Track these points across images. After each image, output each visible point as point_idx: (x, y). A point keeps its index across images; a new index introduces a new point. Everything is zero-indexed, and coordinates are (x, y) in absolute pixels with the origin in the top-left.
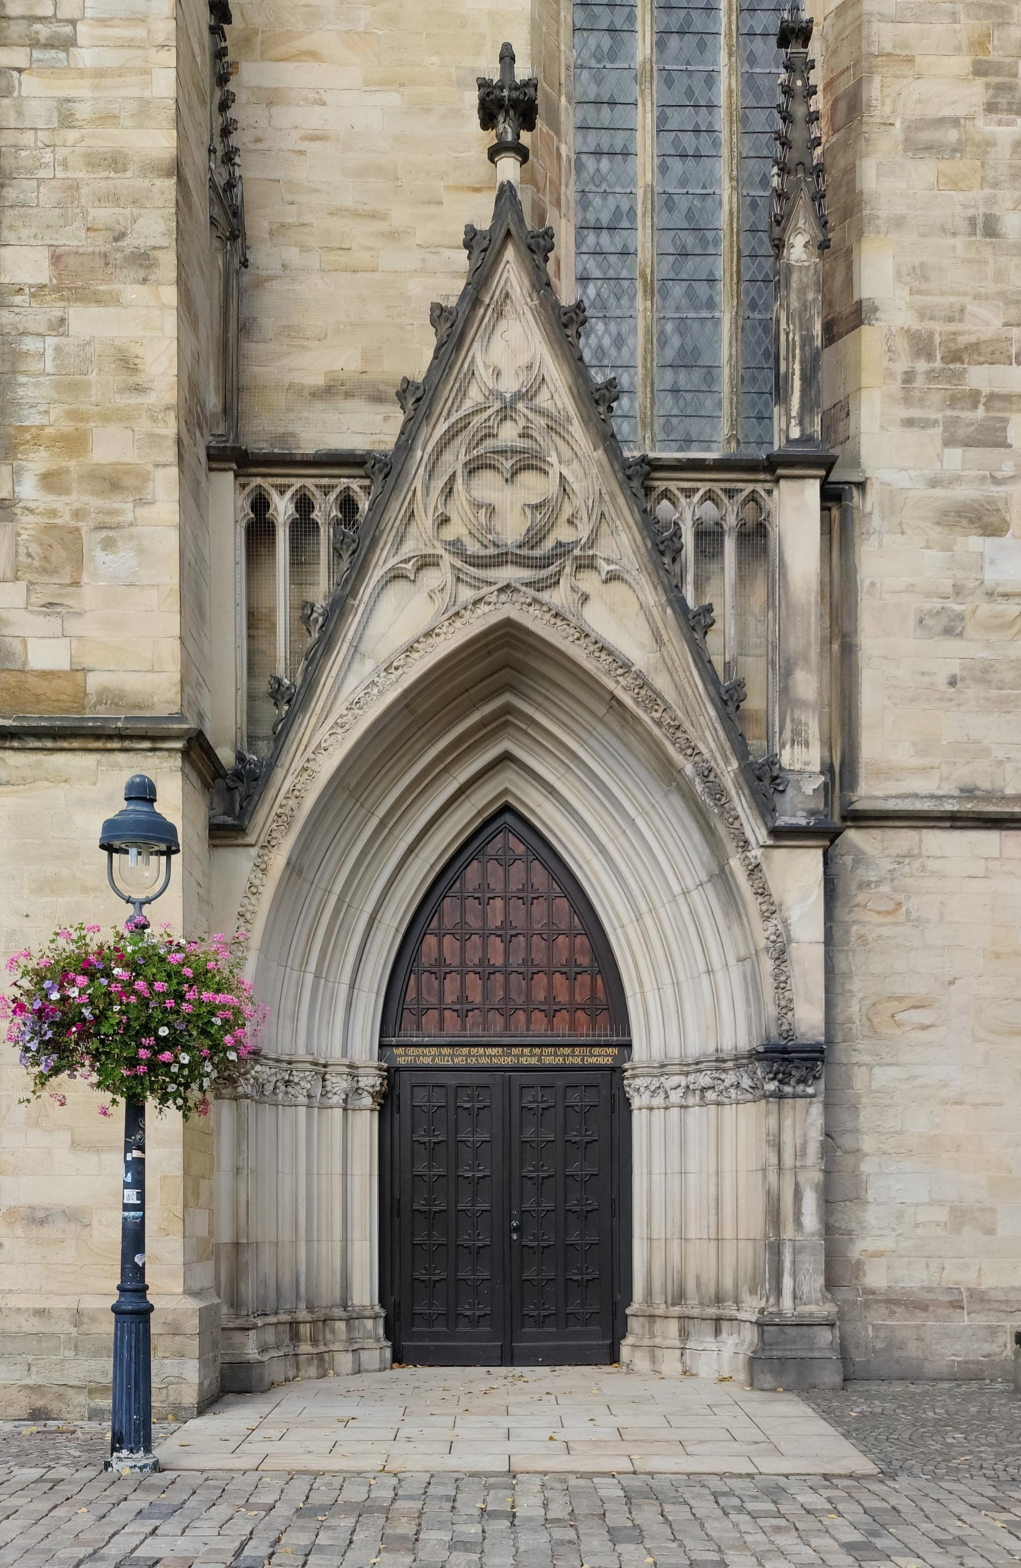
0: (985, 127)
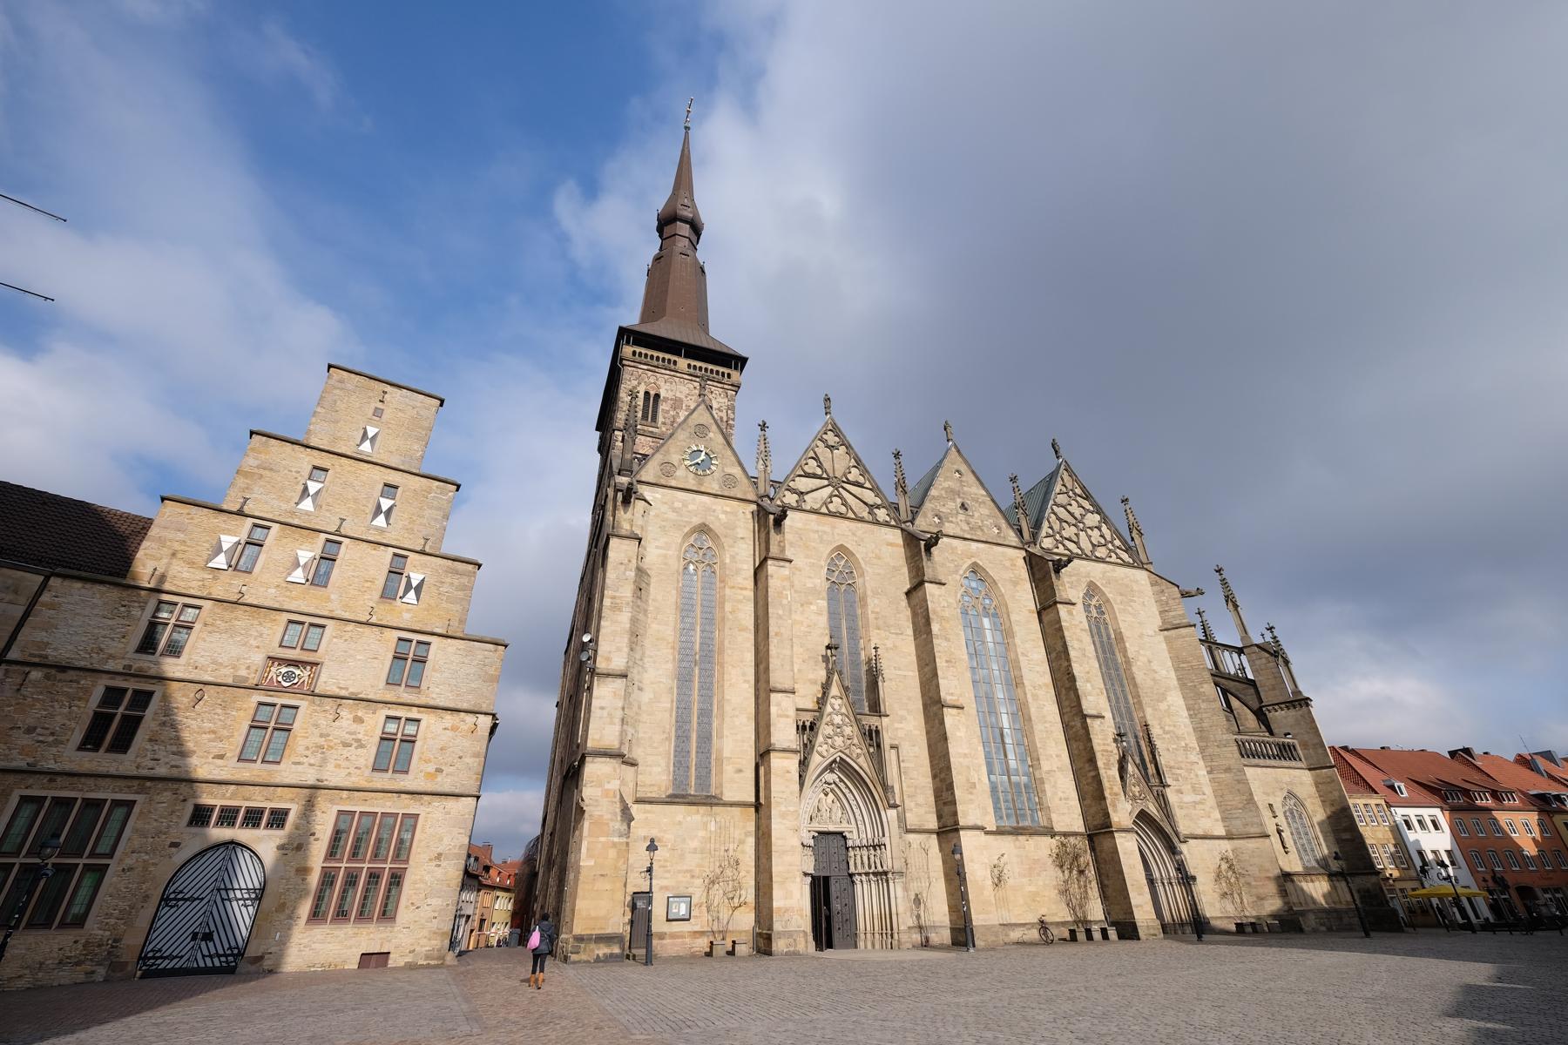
0: (1164, 736)
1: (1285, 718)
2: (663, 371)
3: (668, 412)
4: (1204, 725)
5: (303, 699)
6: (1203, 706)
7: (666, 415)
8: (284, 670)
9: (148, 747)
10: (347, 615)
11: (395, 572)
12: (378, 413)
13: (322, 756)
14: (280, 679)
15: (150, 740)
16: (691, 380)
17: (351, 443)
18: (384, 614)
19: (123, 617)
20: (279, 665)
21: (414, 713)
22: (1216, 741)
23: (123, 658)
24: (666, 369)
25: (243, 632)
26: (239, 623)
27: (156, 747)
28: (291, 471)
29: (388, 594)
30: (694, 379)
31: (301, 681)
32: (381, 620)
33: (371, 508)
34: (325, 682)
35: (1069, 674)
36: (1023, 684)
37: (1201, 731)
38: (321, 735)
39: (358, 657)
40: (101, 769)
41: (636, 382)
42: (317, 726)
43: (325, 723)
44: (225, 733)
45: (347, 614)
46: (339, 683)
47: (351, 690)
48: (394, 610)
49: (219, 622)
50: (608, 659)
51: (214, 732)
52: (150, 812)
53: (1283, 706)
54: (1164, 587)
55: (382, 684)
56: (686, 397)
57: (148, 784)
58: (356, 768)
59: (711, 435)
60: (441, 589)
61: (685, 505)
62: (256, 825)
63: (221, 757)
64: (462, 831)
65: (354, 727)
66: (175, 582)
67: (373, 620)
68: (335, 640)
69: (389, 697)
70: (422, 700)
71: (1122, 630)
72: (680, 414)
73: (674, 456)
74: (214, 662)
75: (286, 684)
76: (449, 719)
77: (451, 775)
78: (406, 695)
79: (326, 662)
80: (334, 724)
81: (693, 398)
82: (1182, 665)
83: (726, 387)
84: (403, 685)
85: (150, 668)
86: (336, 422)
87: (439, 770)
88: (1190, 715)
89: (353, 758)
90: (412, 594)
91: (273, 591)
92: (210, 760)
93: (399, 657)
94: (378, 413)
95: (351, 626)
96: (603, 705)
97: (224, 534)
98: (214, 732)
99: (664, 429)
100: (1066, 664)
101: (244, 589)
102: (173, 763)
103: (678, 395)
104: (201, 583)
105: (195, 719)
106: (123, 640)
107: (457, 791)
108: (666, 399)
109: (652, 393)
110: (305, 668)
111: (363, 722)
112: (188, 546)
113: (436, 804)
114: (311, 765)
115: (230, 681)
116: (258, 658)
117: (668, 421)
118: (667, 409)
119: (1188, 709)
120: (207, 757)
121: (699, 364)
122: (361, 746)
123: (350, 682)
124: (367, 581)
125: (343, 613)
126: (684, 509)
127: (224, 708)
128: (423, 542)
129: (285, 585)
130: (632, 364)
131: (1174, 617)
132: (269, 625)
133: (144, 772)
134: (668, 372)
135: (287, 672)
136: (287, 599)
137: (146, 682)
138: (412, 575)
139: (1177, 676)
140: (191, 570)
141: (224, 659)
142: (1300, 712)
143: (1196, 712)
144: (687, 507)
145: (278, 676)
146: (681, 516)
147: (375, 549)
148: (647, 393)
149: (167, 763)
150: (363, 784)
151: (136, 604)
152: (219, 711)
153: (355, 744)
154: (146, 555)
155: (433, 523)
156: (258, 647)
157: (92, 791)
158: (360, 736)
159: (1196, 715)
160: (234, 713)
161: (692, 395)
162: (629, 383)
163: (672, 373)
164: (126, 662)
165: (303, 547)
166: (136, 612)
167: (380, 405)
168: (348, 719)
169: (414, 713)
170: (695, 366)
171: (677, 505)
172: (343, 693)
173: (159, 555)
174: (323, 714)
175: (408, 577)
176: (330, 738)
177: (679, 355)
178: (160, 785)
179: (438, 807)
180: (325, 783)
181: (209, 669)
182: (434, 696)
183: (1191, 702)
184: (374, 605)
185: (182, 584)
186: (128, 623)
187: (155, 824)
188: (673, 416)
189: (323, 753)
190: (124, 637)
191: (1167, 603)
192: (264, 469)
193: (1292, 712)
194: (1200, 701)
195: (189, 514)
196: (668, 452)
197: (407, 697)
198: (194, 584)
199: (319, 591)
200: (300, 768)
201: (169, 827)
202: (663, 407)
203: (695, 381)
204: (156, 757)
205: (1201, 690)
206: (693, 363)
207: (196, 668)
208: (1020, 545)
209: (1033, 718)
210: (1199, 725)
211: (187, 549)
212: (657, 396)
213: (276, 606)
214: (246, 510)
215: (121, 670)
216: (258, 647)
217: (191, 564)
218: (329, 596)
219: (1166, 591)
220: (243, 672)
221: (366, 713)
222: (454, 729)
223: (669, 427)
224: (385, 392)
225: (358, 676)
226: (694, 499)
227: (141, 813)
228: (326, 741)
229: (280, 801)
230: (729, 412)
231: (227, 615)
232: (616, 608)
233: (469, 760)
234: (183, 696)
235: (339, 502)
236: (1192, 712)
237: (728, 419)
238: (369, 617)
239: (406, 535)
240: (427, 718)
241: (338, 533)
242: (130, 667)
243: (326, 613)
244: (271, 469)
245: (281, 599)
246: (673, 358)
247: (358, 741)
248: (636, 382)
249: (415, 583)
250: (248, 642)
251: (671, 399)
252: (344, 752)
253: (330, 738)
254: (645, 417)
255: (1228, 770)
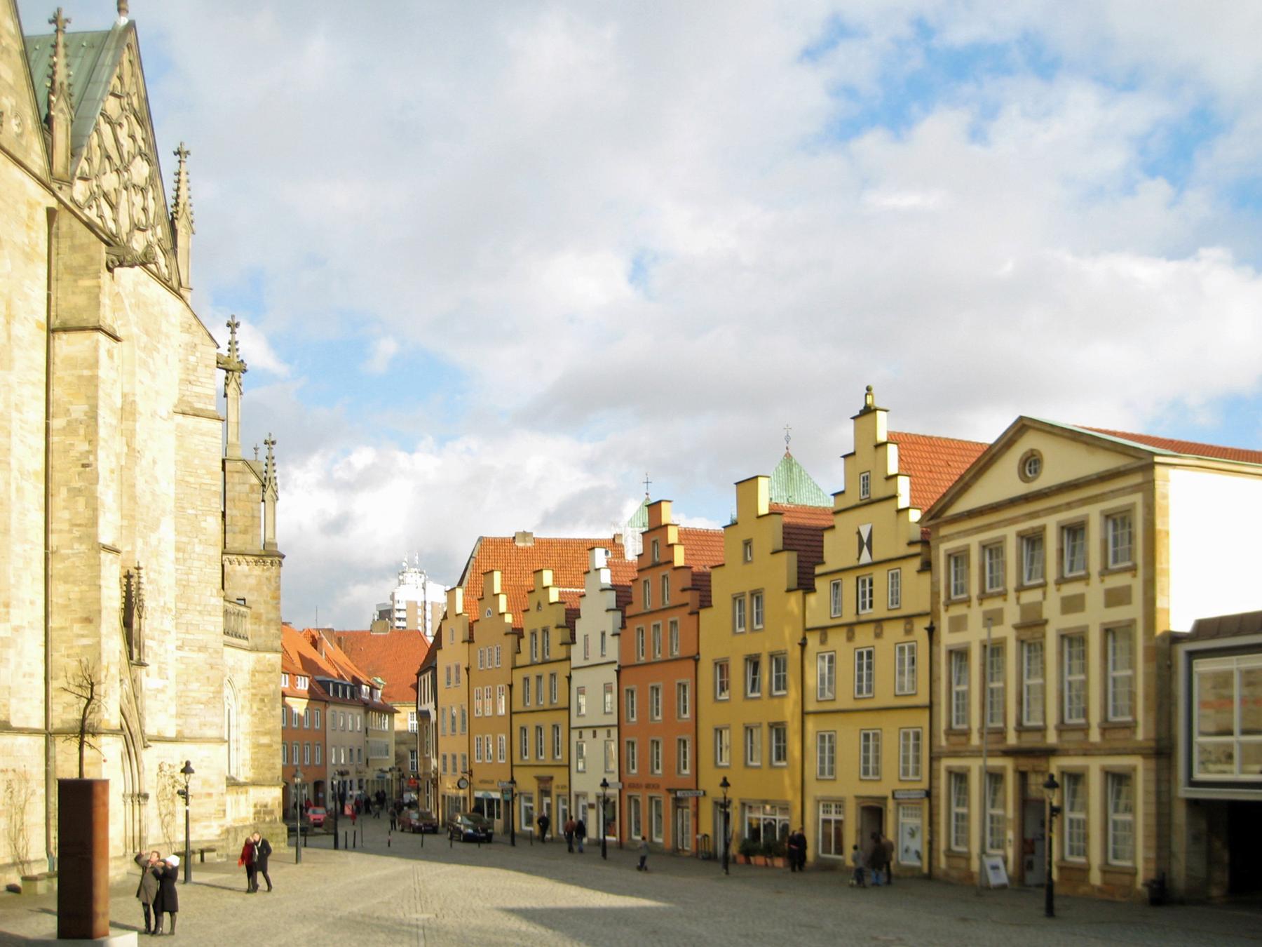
1: (247, 576)
4: (192, 577)
6: (198, 549)
22: (200, 605)
35: (84, 466)
36: (9, 464)
37: (184, 586)
53: (249, 558)
54: (197, 341)
71: (137, 399)
82: (188, 479)
88: (177, 559)
100: (86, 447)
119: (178, 549)
131: (198, 396)
139: (176, 494)
142: (267, 574)
143: (186, 556)
159: (185, 560)
183: (185, 539)
191: (195, 370)
193: (258, 571)
194: (196, 540)
205: (203, 524)
208: (45, 176)
209: (13, 532)
210: (185, 577)
219: (200, 347)
236: (180, 555)
255: (202, 649)
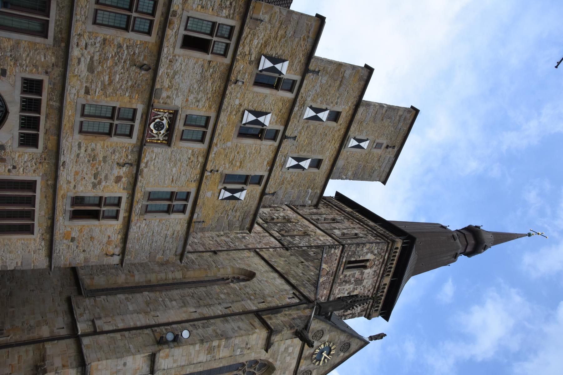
2: (382, 269)
3: (353, 276)
5: (138, 139)
7: (351, 276)
8: (165, 122)
9: (98, 39)
10: (212, 156)
11: (246, 180)
12: (379, 146)
13: (86, 161)
14: (157, 120)
15: (105, 40)
16: (375, 288)
17: (357, 133)
18: (211, 181)
19: (221, 5)
20: (170, 118)
21: (122, 215)
23: (183, 10)
24: (384, 271)
25: (202, 88)
26: (210, 84)
27: (98, 45)
28: (338, 99)
29: (229, 179)
30: (376, 289)
31: (156, 135)
32: (206, 178)
33: (302, 154)
34: (153, 151)
38: (105, 158)
39: (174, 169)
40: (79, 9)
41: (376, 252)
42: (114, 152)
43: (116, 157)
44: (110, 90)
45: (213, 155)
46: (151, 161)
47: (145, 170)
48: (215, 185)
49: (211, 70)
50: (167, 356)
51: (111, 82)
52: (36, 50)
55: (149, 189)
56: (363, 286)
57: (63, 45)
58: (75, 186)
59: (342, 354)
60: (231, 211)
61: (289, 354)
62: (22, 126)
63: (87, 92)
64: (19, 264)
65: (112, 178)
66: (250, 36)
67: (207, 174)
68: (190, 151)
69: (138, 195)
70: (134, 218)
72: (352, 286)
73: (328, 336)
74: (175, 73)
75: (152, 126)
76: (117, 238)
77: (69, 248)
78: (140, 206)
79: (169, 150)
80: (115, 163)
81: (362, 291)
83: (368, 310)
84: (148, 203)
85: (172, 29)
86: (374, 121)
87: (73, 240)
89: (84, 182)
90: (228, 194)
91: (237, 102)
92: (85, 85)
93: (172, 196)
94: (379, 146)
95: (201, 159)
96: (128, 364)
97: (289, 63)
98: (111, 82)
99: (341, 277)
101: (240, 83)
102: (82, 59)
103: (365, 281)
104: (247, 53)
105: (123, 68)
106: (200, 7)
107: (54, 255)
108: (362, 273)
109: (368, 264)
110: (166, 136)
111: (116, 183)
112: (280, 40)
113: (43, 244)
114: (78, 155)
115: (158, 86)
116: (178, 102)
117: (347, 278)
118: (356, 276)
120: (86, 82)
121: (385, 290)
122: (94, 186)
123: (152, 168)
124: (241, 163)
125: (213, 153)
126: (287, 355)
127: (132, 86)
128: (272, 191)
129: (242, 109)
130: (389, 249)
132: (207, 105)
133: (74, 40)
134: (381, 272)
135: (163, 124)
136: (229, 113)
137: (159, 28)
138: (244, 192)
140: (260, 45)
141: (177, 79)
144: (289, 355)
145: (160, 118)
146: (282, 354)
147: (268, 163)
148: (367, 260)
149: (82, 55)
150: (60, 193)
151: (232, 12)
152: (130, 83)
153: (96, 181)
154: (275, 13)
155: (287, 196)
156: (187, 100)
157: (58, 5)
158: (103, 183)
160: (127, 94)
161: (364, 290)
162: (376, 248)
163: (380, 275)
164: (179, 12)
165: (274, 116)
166: (225, 12)
167: (384, 145)
168: (118, 172)
169: (122, 215)
170: (385, 288)
171: (290, 350)
172: (143, 165)
173: (274, 21)
174: (124, 154)
175: (242, 190)
176: (102, 164)
177: (393, 277)
178: (61, 53)
179: (40, 245)
180: (62, 168)
181: (169, 71)
182: (138, 225)
184: (219, 172)
185: (248, 40)
186: (216, 8)
187: (24, 56)
188: (350, 281)
189: (89, 161)
190: (202, 7)
192: (341, 81)
195: (308, 37)
196: (330, 331)
197: (137, 208)
198: (247, 49)
199: (235, 131)
200: (75, 148)
201: (21, 65)
202: (357, 273)
203: (374, 290)
204: (89, 47)
206: (387, 287)
207: (170, 61)
211: (278, 39)
212: (365, 267)
213: (224, 107)
214: (310, 76)
215: (172, 10)
216: (187, 100)
217: (266, 44)
218: (229, 141)
220: (164, 94)
221: (124, 184)
222: (109, 243)
223: (343, 280)
224: (394, 147)
225: (158, 173)
226: (294, 358)
227: (35, 44)
228: (100, 161)
229: (45, 139)
230: (351, 315)
231: (217, 75)
232: (210, 350)
233: (82, 256)
234: (145, 56)
235: (310, 133)
237: (346, 316)
238: (209, 170)
239: (278, 181)
240: (117, 224)
241: (284, 137)
242: (174, 15)
243: (215, 141)
244: (340, 85)
245: (229, 109)
246: (391, 274)
247: (100, 183)
248: (376, 252)
249: (237, 195)
250: (192, 93)
251: (362, 277)
252: (89, 175)
253: (102, 164)
254: (350, 262)
